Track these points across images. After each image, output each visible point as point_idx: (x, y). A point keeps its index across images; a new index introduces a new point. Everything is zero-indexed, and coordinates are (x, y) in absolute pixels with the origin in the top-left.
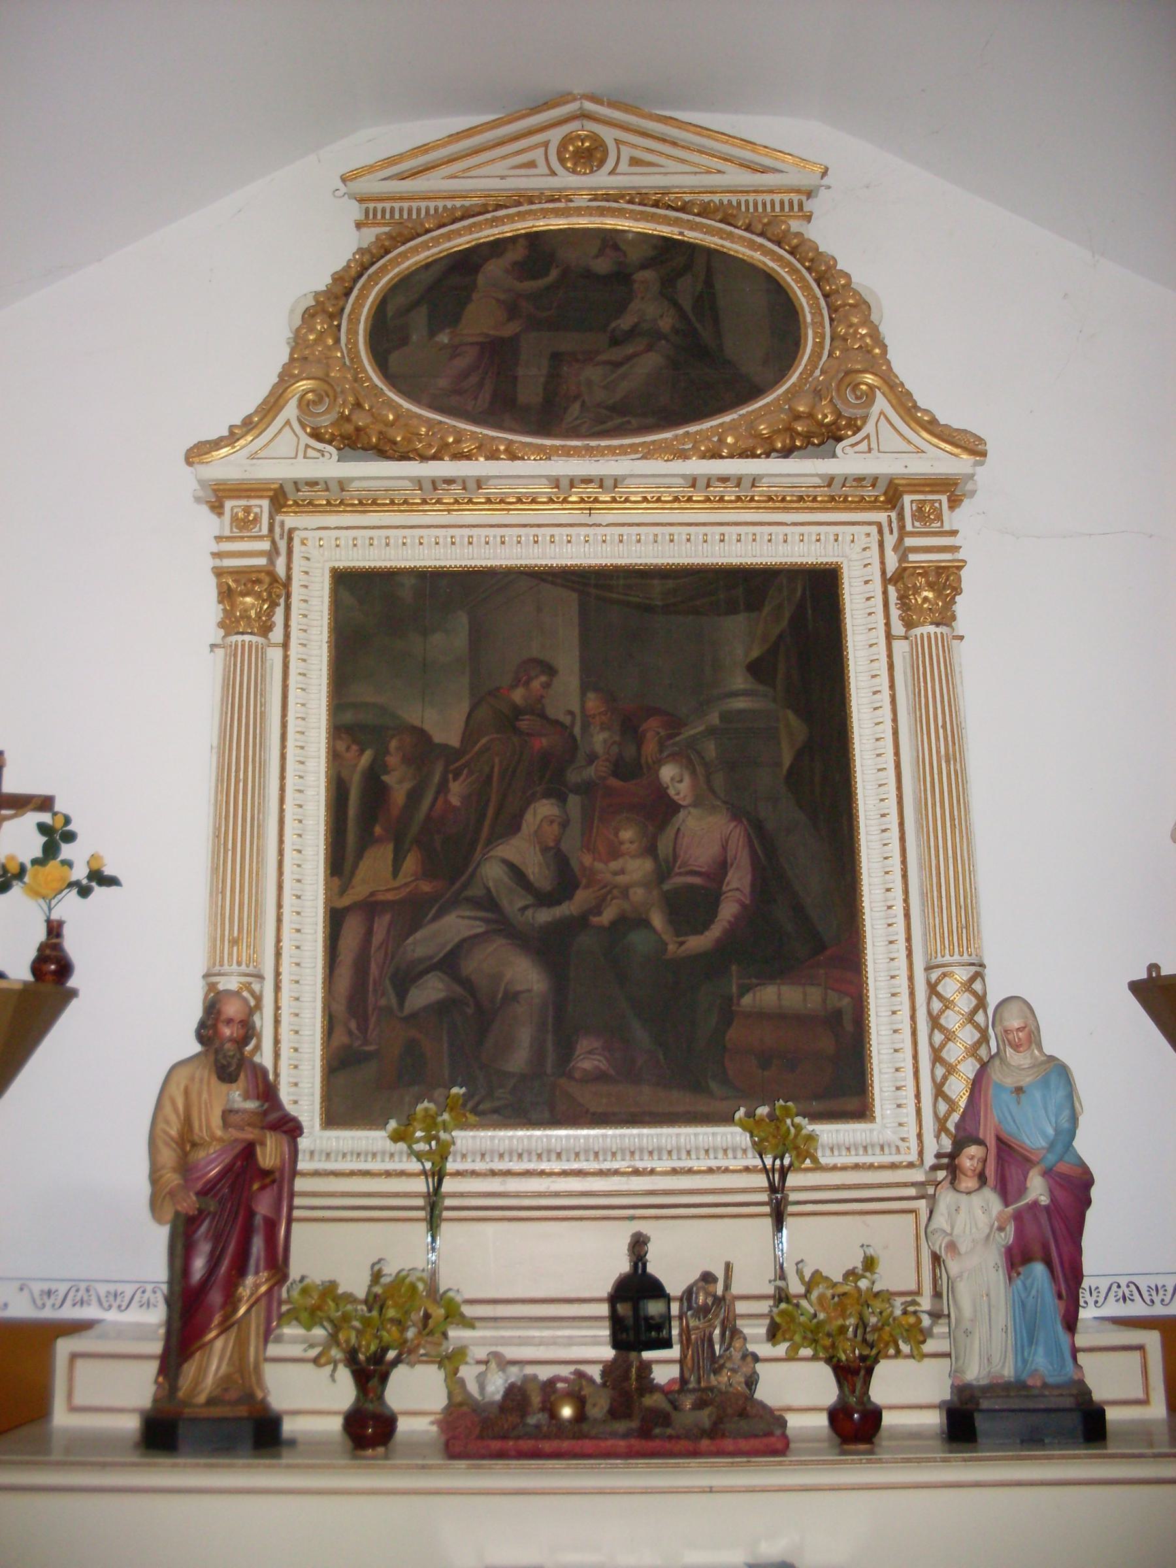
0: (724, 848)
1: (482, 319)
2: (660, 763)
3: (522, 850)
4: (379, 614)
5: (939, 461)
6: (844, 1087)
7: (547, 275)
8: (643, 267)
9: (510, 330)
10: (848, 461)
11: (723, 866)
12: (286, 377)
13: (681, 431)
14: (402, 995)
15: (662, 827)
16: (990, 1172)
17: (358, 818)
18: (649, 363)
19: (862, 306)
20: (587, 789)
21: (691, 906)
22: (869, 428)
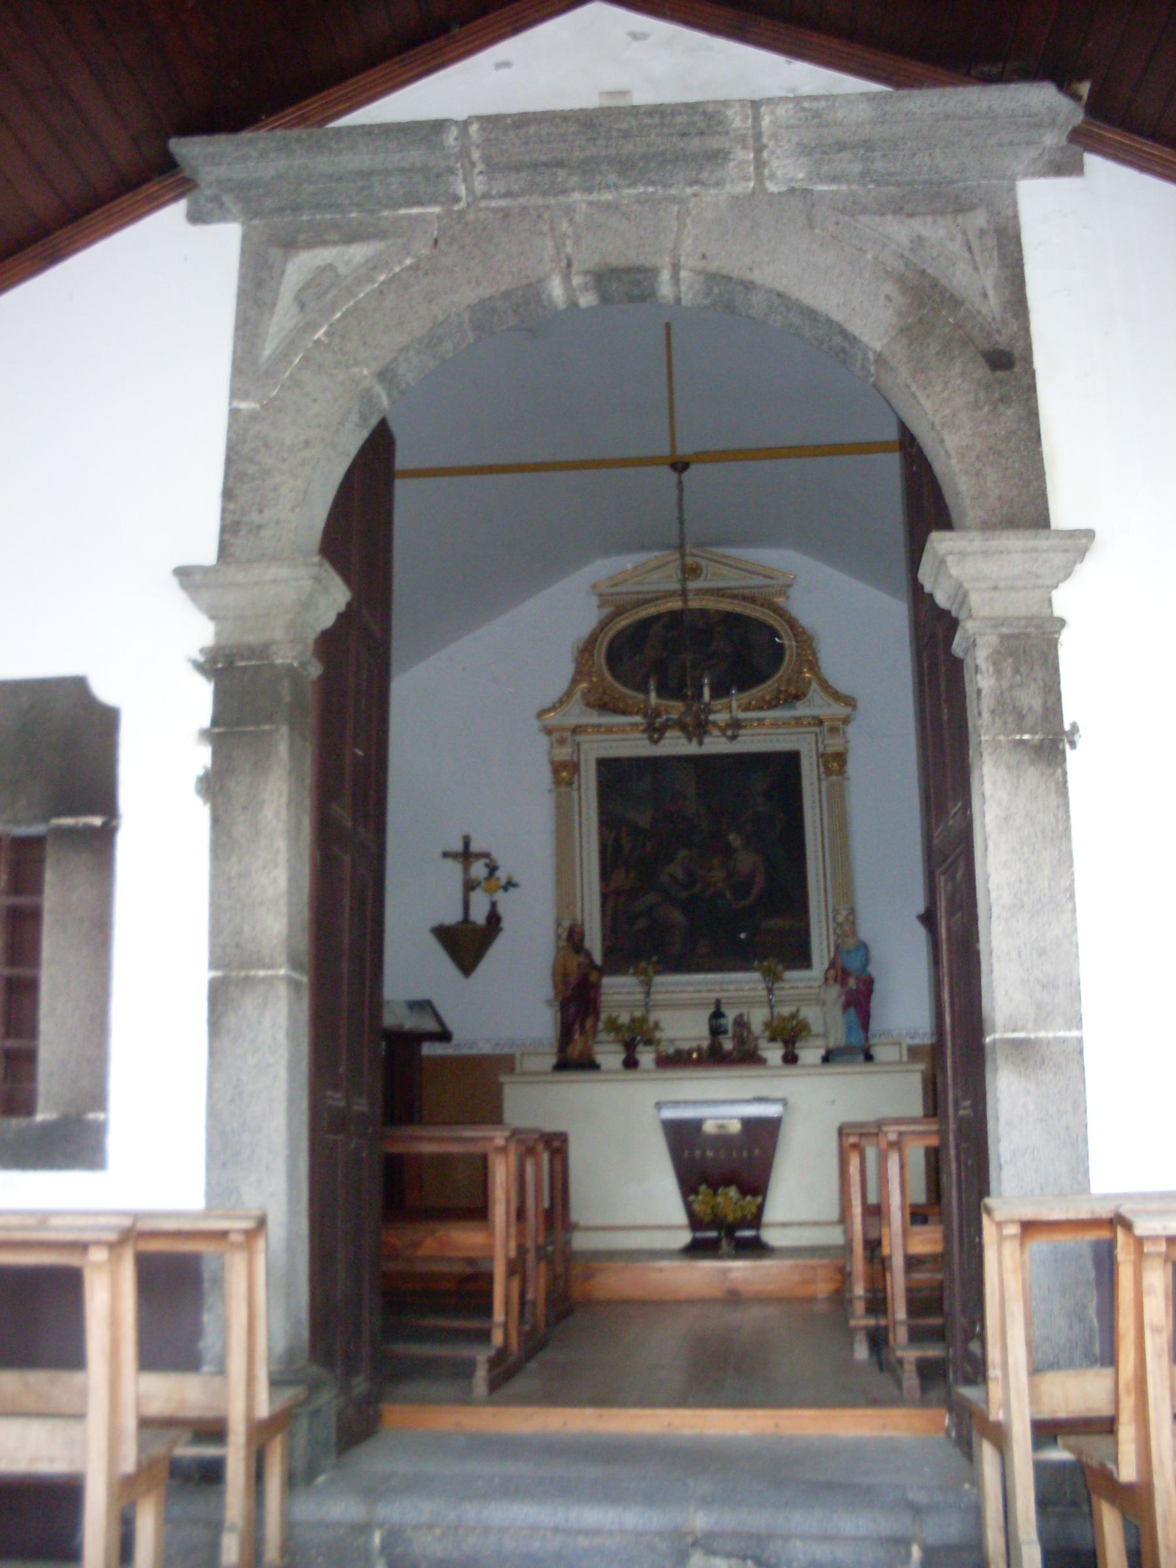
4: (616, 776)
6: (802, 959)
10: (802, 710)
12: (575, 682)
16: (839, 979)
17: (611, 859)
22: (810, 694)
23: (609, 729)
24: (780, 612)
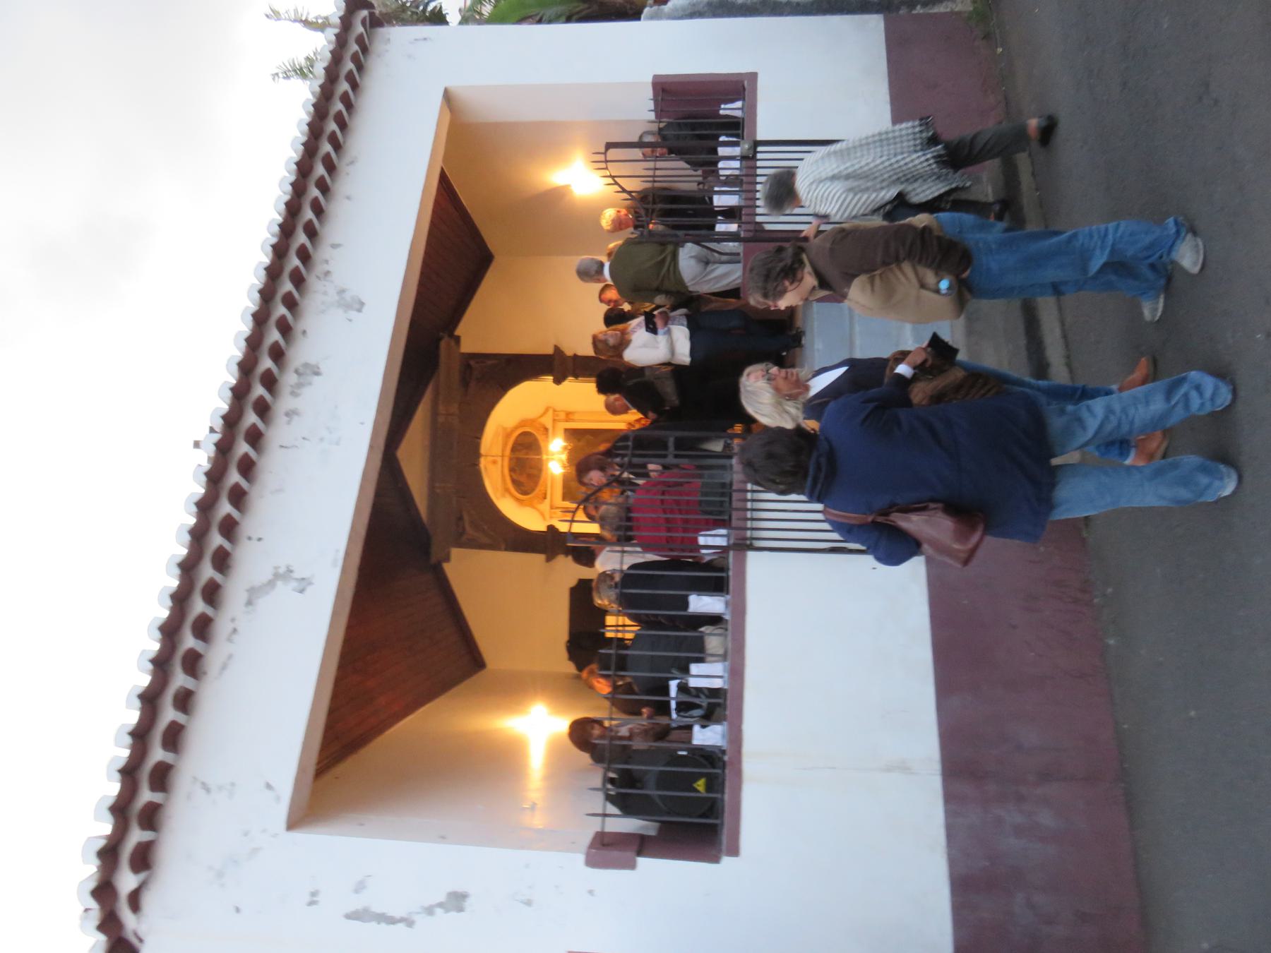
1: (523, 479)
10: (549, 426)
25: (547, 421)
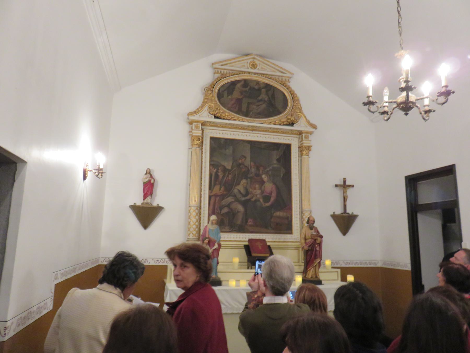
0: (272, 188)
1: (236, 94)
2: (262, 175)
3: (241, 188)
4: (218, 145)
5: (310, 129)
7: (247, 87)
8: (263, 88)
9: (241, 97)
11: (271, 193)
13: (269, 119)
14: (221, 211)
15: (262, 185)
18: (264, 106)
19: (298, 100)
20: (251, 178)
21: (267, 198)
23: (216, 125)
24: (288, 88)
25: (300, 126)
